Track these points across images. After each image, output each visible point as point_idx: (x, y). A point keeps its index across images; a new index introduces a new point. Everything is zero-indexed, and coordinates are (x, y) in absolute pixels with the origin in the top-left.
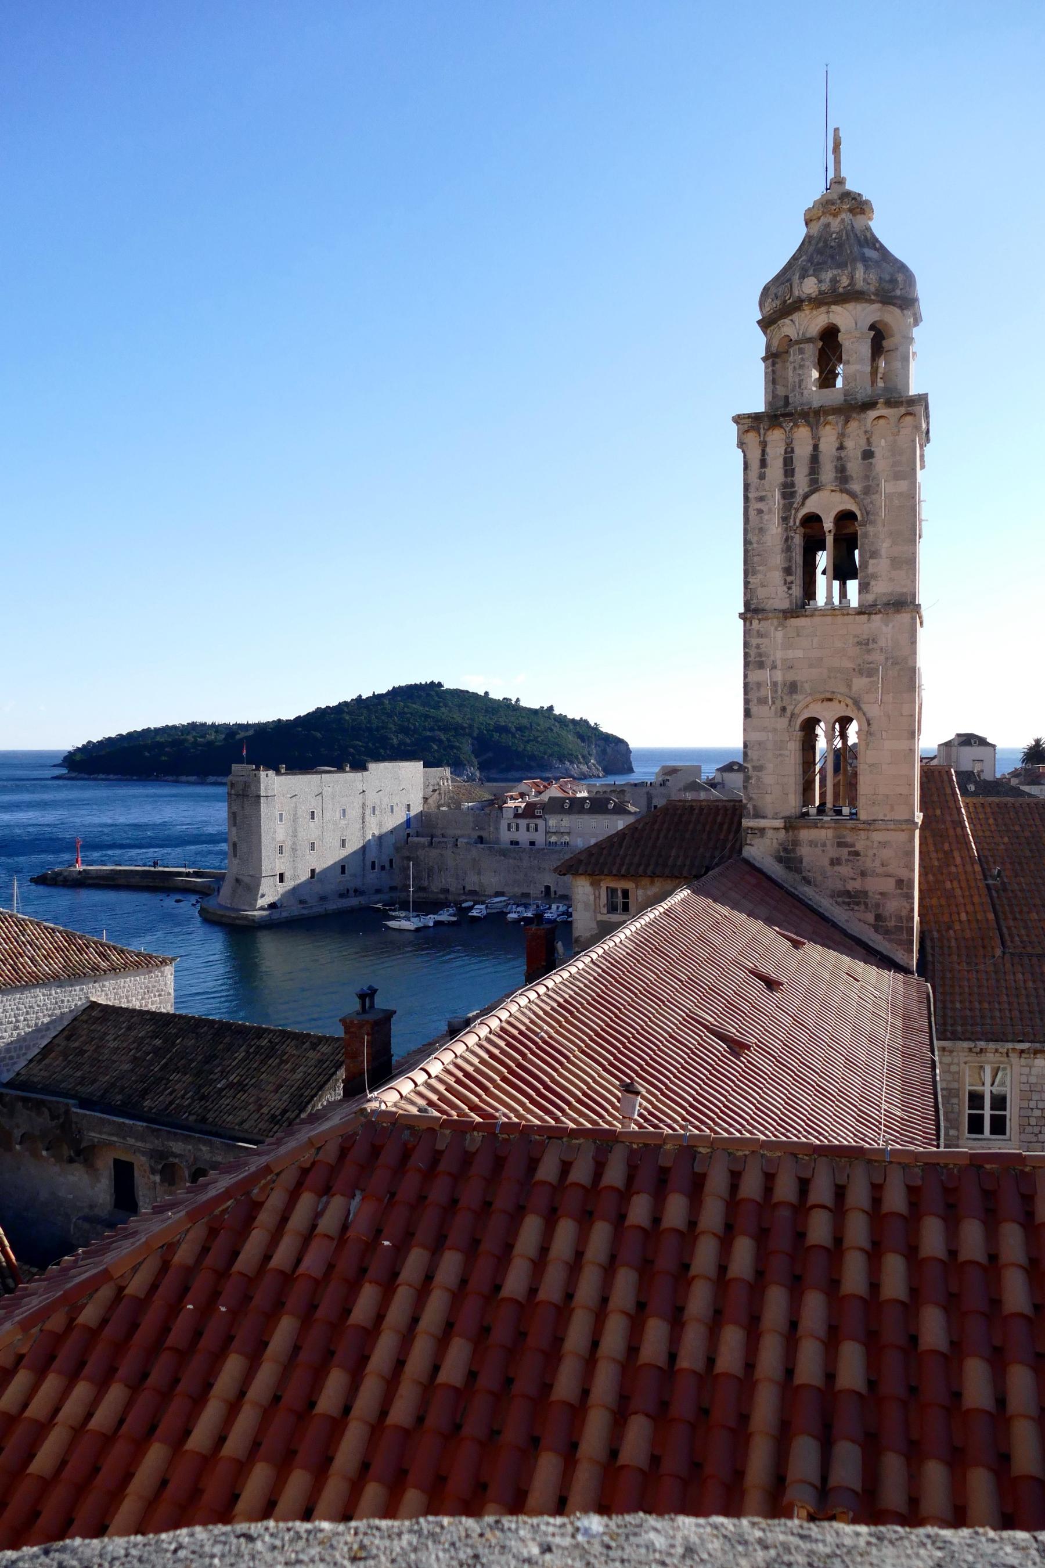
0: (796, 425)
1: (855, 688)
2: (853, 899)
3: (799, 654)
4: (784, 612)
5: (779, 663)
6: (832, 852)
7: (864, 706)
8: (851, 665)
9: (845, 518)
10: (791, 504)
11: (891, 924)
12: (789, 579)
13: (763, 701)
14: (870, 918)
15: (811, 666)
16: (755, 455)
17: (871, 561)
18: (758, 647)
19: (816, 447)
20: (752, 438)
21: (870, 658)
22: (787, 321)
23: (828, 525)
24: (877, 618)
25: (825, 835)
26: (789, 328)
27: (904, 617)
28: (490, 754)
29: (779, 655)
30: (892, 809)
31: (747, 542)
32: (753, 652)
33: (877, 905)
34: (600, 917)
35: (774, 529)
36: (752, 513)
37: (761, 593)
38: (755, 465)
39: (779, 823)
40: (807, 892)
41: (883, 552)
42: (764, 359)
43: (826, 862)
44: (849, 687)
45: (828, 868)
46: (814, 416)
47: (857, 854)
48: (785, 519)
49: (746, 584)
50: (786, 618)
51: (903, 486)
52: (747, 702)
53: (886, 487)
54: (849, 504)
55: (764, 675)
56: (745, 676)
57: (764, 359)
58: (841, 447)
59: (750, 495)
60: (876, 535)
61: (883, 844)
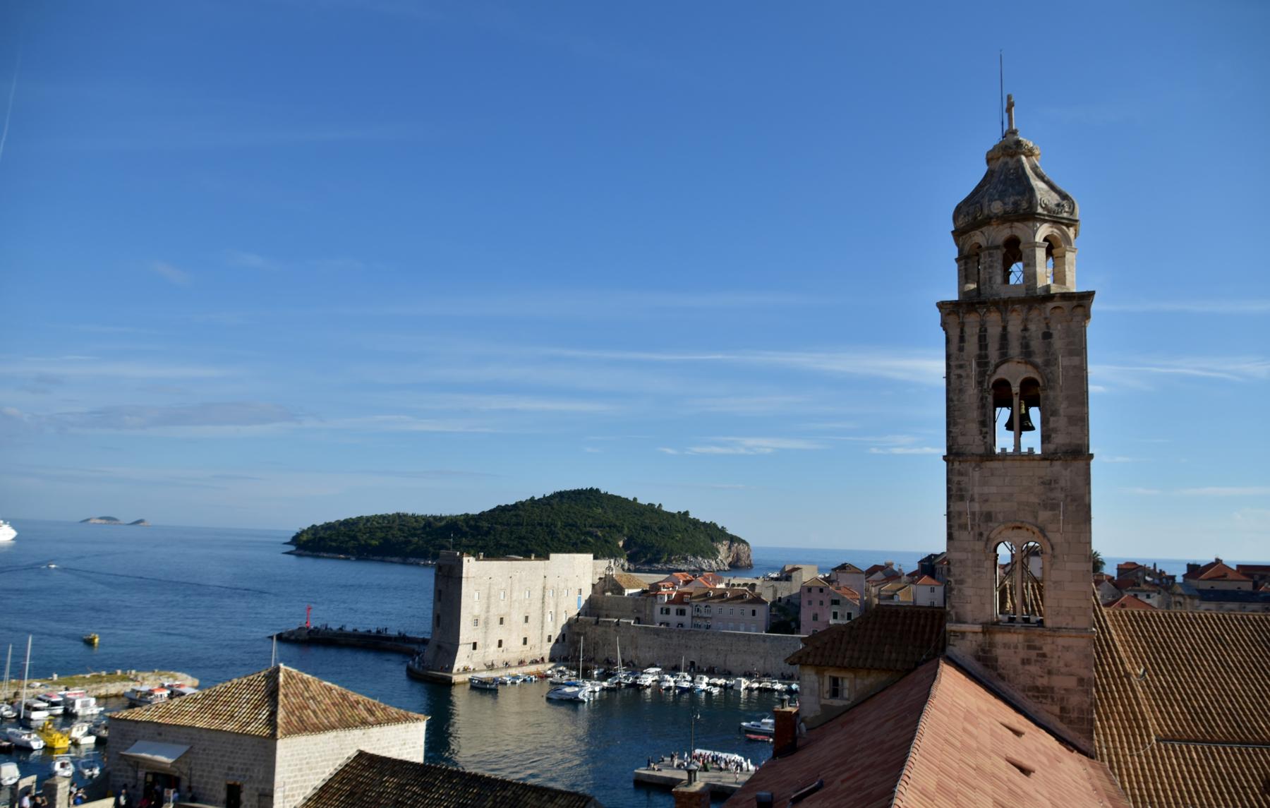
0: (988, 310)
1: (1040, 519)
2: (1042, 693)
3: (993, 490)
4: (981, 456)
5: (976, 496)
6: (1023, 653)
7: (1049, 535)
8: (1037, 501)
10: (985, 372)
11: (1074, 715)
12: (984, 430)
13: (963, 527)
14: (1056, 710)
15: (1003, 500)
16: (955, 333)
17: (1052, 419)
18: (959, 483)
19: (1005, 328)
20: (953, 319)
21: (1052, 495)
22: (978, 232)
23: (1016, 389)
24: (1058, 465)
25: (1016, 638)
26: (978, 238)
27: (1081, 464)
28: (634, 549)
29: (976, 490)
30: (1074, 619)
31: (949, 400)
32: (954, 488)
33: (1062, 699)
34: (823, 702)
35: (972, 391)
36: (953, 377)
37: (961, 440)
38: (955, 340)
39: (978, 628)
40: (1003, 685)
41: (1062, 412)
42: (957, 260)
43: (1018, 661)
44: (1036, 517)
45: (1020, 667)
46: (1004, 305)
47: (1044, 655)
48: (980, 383)
49: (949, 433)
50: (982, 461)
51: (1076, 360)
52: (949, 527)
53: (1063, 361)
54: (1031, 373)
55: (965, 506)
56: (948, 507)
57: (957, 260)
58: (1025, 329)
59: (952, 364)
61: (1067, 648)
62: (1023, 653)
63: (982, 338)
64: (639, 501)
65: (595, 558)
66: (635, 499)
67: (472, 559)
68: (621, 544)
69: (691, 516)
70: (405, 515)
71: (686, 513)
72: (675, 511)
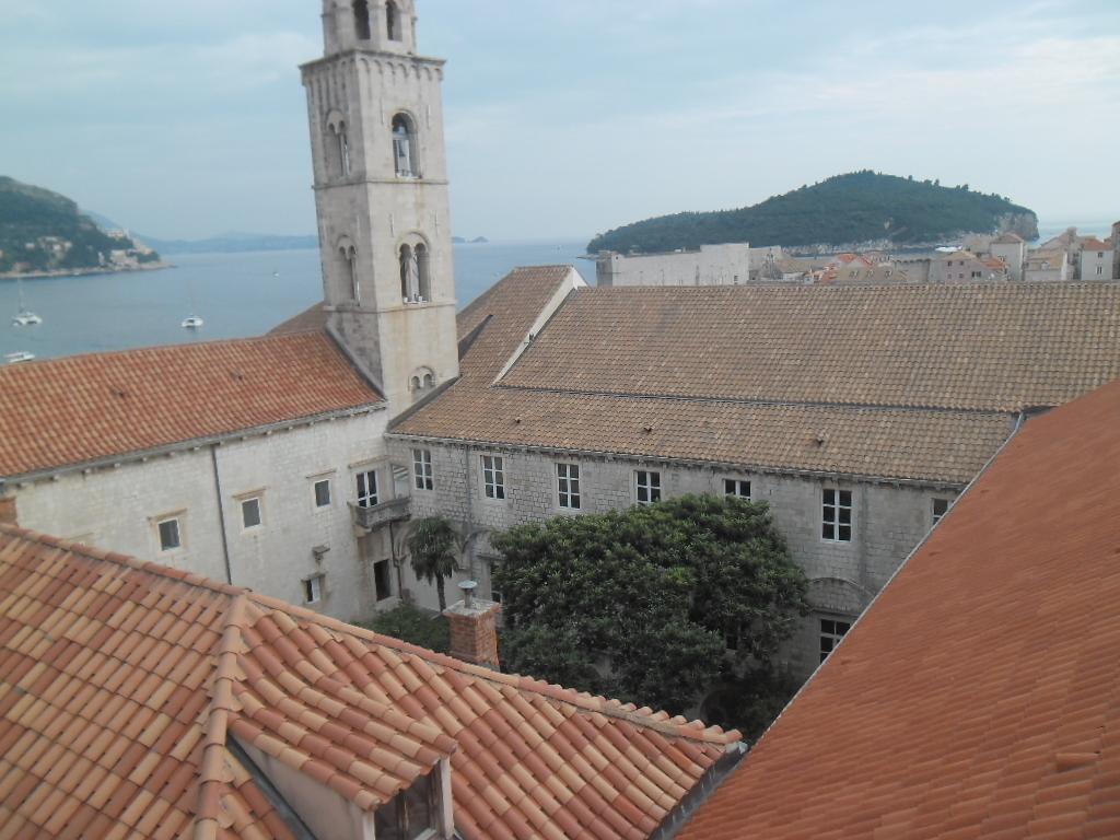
2: (362, 351)
9: (342, 124)
27: (362, 186)
31: (312, 143)
47: (360, 327)
55: (325, 223)
60: (351, 133)
63: (320, 92)
64: (915, 179)
66: (910, 177)
67: (620, 256)
68: (887, 225)
69: (971, 190)
70: (642, 222)
71: (966, 187)
72: (954, 186)
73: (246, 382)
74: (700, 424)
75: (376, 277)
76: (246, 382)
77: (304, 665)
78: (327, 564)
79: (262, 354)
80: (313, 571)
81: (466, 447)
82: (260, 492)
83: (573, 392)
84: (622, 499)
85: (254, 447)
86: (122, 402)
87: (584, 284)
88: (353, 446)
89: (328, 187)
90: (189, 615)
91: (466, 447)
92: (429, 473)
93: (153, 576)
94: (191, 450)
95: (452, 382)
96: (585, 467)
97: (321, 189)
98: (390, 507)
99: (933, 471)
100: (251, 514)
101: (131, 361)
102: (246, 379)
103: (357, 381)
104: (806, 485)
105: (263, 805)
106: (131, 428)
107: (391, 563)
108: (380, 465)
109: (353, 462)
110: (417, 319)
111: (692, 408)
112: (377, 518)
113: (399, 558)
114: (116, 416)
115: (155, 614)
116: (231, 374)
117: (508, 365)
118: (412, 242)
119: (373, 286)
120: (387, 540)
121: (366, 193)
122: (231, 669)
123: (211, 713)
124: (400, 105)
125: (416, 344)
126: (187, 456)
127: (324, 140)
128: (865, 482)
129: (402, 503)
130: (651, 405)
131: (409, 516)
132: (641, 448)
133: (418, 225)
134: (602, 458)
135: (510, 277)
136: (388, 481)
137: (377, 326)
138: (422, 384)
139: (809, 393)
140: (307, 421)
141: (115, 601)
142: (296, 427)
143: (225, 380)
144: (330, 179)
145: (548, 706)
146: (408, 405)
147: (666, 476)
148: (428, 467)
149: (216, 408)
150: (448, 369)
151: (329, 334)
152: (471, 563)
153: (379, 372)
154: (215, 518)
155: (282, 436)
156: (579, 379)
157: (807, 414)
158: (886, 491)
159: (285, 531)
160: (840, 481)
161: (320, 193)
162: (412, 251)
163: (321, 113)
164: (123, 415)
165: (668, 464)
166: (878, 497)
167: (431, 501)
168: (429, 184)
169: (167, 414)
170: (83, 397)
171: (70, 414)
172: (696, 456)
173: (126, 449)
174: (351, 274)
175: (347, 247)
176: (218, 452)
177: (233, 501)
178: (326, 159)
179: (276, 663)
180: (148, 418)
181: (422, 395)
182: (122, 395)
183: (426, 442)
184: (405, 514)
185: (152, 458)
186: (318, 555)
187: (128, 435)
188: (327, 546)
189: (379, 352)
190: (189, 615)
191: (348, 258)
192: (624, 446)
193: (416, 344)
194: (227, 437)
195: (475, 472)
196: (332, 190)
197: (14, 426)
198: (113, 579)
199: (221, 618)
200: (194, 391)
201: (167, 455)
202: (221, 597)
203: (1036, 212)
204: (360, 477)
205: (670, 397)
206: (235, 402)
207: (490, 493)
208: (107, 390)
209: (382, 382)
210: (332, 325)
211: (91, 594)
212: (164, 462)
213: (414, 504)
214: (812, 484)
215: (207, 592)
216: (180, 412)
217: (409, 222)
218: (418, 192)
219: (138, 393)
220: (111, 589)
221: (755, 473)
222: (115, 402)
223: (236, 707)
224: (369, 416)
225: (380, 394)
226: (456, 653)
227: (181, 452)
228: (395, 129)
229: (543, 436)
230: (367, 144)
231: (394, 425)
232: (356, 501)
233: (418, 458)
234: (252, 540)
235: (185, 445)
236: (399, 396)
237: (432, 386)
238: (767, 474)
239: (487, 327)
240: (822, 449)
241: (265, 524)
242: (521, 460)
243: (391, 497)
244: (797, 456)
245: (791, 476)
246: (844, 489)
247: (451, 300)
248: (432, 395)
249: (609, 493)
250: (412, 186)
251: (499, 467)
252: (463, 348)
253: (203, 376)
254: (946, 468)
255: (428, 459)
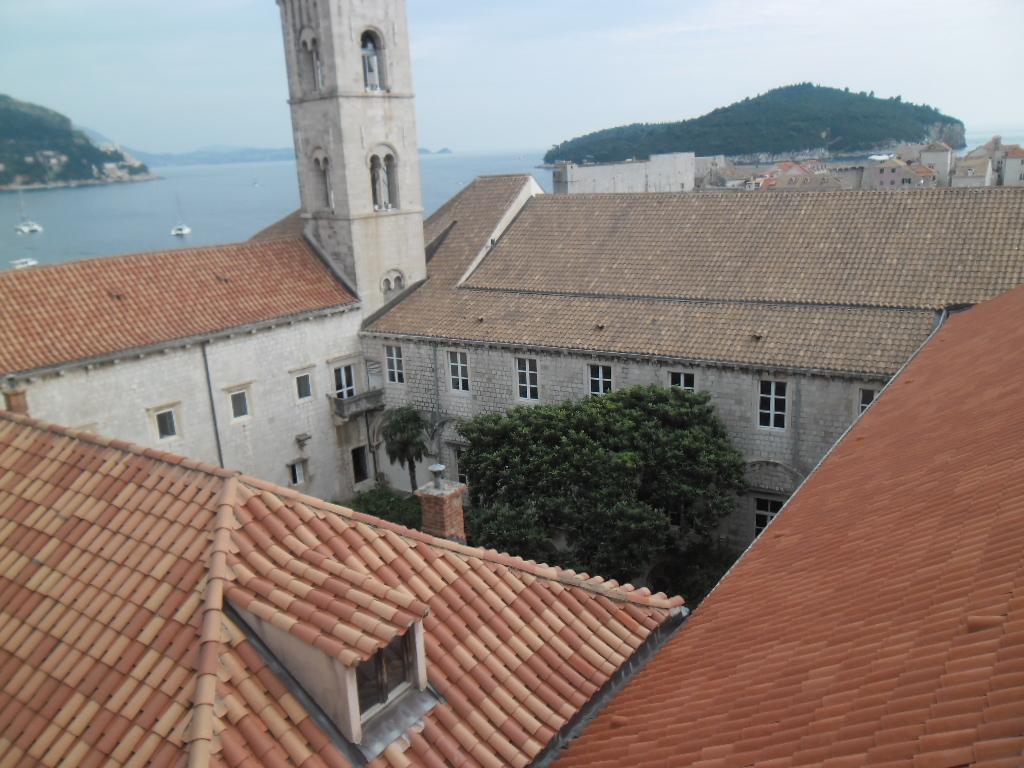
2: (337, 256)
9: (315, 42)
27: (334, 100)
28: (838, 138)
40: (323, 252)
47: (335, 232)
53: (323, 24)
55: (300, 135)
60: (322, 49)
62: (330, 232)
64: (851, 91)
65: (696, 156)
66: (847, 89)
67: (575, 165)
68: (824, 135)
71: (899, 98)
72: (887, 97)
73: (231, 285)
74: (648, 322)
75: (349, 186)
76: (231, 285)
77: (291, 540)
78: (309, 451)
79: (246, 259)
80: (297, 456)
81: (434, 344)
82: (247, 385)
83: (530, 293)
84: (576, 390)
85: (239, 345)
86: (119, 304)
87: (541, 192)
88: (331, 343)
89: (302, 101)
90: (186, 495)
91: (434, 344)
92: (400, 367)
93: (153, 461)
94: (183, 347)
95: (420, 284)
96: (541, 361)
97: (295, 103)
98: (366, 398)
99: (862, 364)
100: (239, 405)
101: (125, 266)
102: (232, 282)
103: (332, 283)
104: (744, 377)
105: (256, 661)
106: (128, 327)
107: (367, 450)
108: (355, 361)
109: (330, 358)
110: (387, 225)
111: (641, 306)
112: (354, 409)
113: (375, 444)
114: (114, 316)
115: (155, 494)
116: (218, 278)
117: (472, 268)
118: (382, 153)
119: (346, 195)
120: (363, 429)
121: (338, 107)
122: (225, 544)
123: (209, 582)
124: (368, 23)
125: (387, 249)
126: (180, 353)
127: (298, 57)
128: (798, 374)
129: (376, 395)
130: (603, 304)
131: (383, 406)
132: (594, 343)
133: (387, 136)
134: (558, 353)
135: (473, 186)
136: (363, 374)
137: (350, 232)
138: (393, 285)
139: (749, 292)
140: (288, 320)
141: (119, 483)
142: (279, 325)
143: (212, 283)
144: (305, 94)
145: (510, 576)
146: (380, 304)
147: (617, 369)
148: (399, 362)
149: (205, 309)
150: (416, 272)
151: (306, 240)
152: (440, 449)
153: (352, 275)
154: (208, 409)
155: (266, 334)
156: (536, 281)
157: (746, 312)
158: (818, 382)
159: (271, 420)
160: (776, 373)
161: (296, 107)
162: (382, 162)
163: (295, 31)
164: (120, 316)
165: (619, 358)
166: (811, 388)
167: (403, 393)
168: (397, 97)
169: (161, 315)
170: (83, 300)
171: (71, 314)
172: (644, 351)
173: (123, 347)
174: (326, 183)
175: (321, 158)
176: (208, 349)
177: (223, 394)
178: (300, 75)
179: (264, 537)
180: (143, 318)
181: (393, 296)
182: (118, 297)
183: (397, 339)
184: (380, 404)
185: (149, 355)
186: (301, 442)
187: (125, 333)
188: (308, 434)
189: (352, 255)
190: (186, 495)
191: (322, 168)
192: (578, 342)
193: (387, 249)
194: (215, 335)
195: (442, 366)
196: (305, 105)
197: (22, 326)
198: (117, 464)
199: (215, 498)
200: (184, 293)
201: (161, 352)
202: (215, 479)
203: (961, 120)
204: (338, 372)
205: (620, 297)
206: (221, 303)
207: (456, 385)
208: (104, 293)
209: (356, 284)
210: (309, 232)
211: (98, 477)
212: (158, 358)
213: (387, 395)
214: (750, 376)
215: (202, 475)
216: (172, 312)
217: (378, 134)
218: (386, 105)
219: (133, 295)
220: (116, 472)
221: (698, 366)
222: (112, 304)
223: (230, 577)
224: (345, 316)
225: (354, 295)
226: (427, 530)
227: (174, 349)
228: (364, 46)
229: (505, 334)
230: (338, 60)
231: (367, 324)
232: (334, 393)
233: (390, 353)
234: (242, 429)
235: (177, 343)
236: (372, 298)
237: (402, 287)
238: (709, 367)
239: (451, 232)
240: (760, 344)
241: (253, 414)
242: (484, 355)
243: (366, 390)
244: (739, 353)
245: (732, 369)
246: (779, 380)
247: (418, 208)
248: (402, 295)
249: (564, 385)
250: (380, 100)
251: (464, 360)
252: (430, 252)
253: (192, 280)
254: (873, 362)
255: (399, 354)
